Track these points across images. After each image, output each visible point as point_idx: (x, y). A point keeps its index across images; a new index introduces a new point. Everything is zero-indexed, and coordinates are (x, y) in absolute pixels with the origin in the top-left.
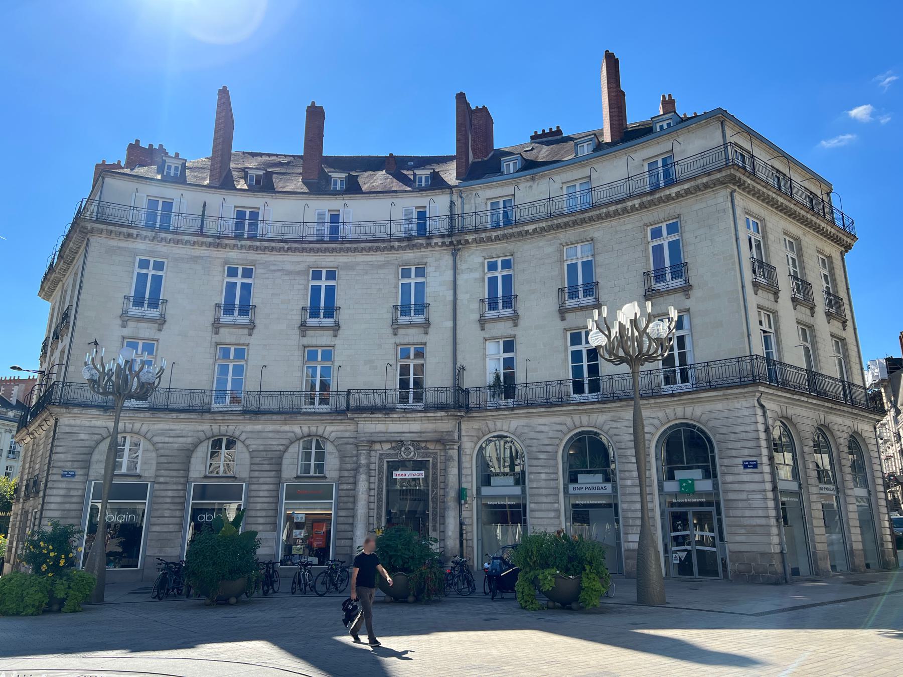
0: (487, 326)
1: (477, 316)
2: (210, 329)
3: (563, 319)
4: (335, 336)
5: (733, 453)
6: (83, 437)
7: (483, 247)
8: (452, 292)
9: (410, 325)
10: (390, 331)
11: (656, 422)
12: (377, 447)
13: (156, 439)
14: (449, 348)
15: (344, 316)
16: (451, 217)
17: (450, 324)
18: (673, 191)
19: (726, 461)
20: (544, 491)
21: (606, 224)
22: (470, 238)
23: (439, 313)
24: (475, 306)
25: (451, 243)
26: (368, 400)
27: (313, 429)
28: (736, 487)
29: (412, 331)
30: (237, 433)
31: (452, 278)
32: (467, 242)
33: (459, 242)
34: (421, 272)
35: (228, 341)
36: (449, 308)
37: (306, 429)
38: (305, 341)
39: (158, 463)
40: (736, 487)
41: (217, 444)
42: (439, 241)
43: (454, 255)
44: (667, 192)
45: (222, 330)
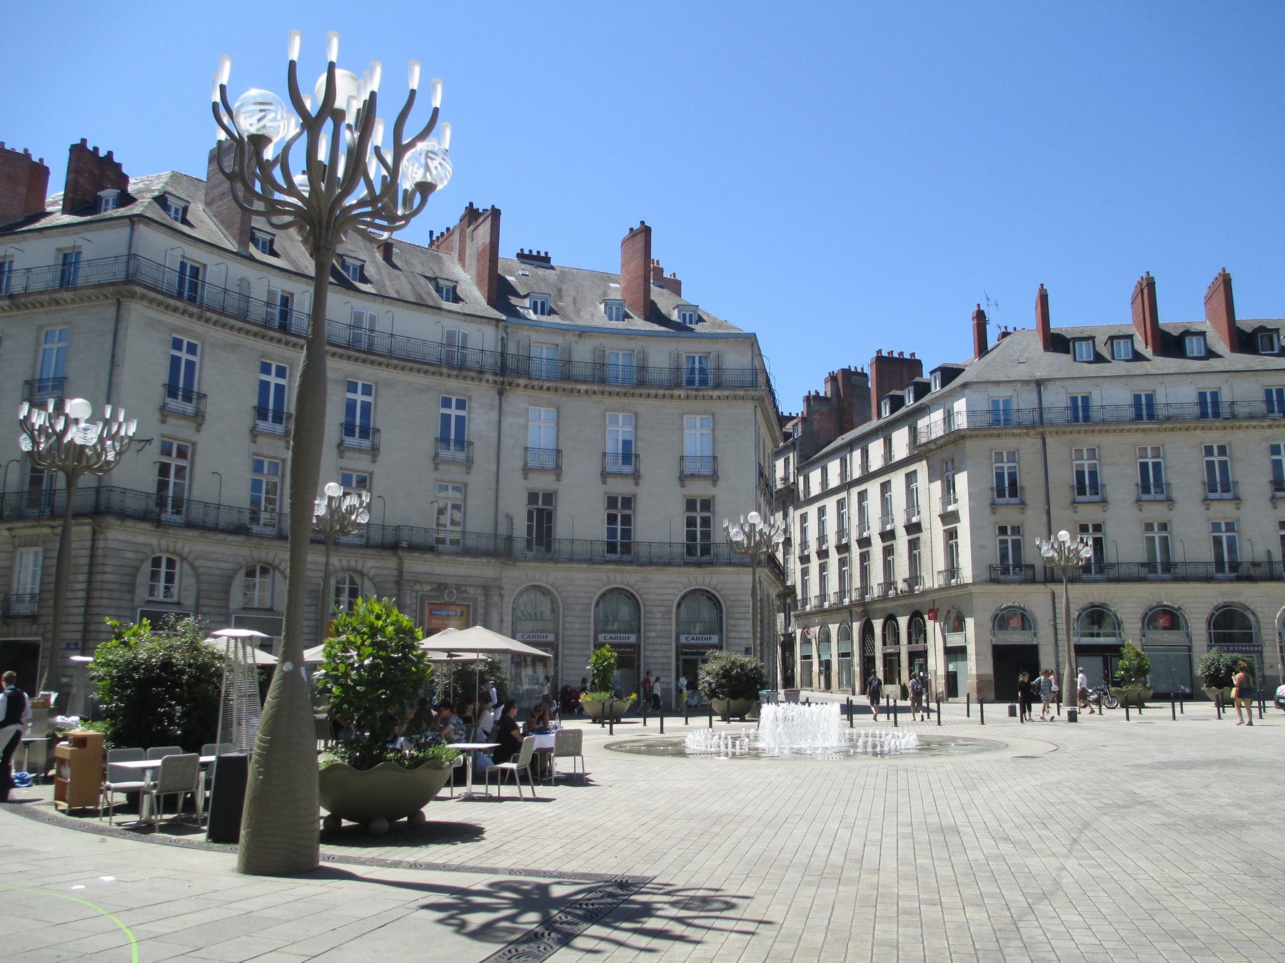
0: (531, 475)
1: (520, 464)
2: (247, 435)
3: (604, 482)
4: (374, 462)
5: (738, 616)
6: (129, 555)
7: (530, 392)
8: (496, 434)
9: (453, 462)
10: (432, 465)
11: (680, 586)
12: (418, 587)
13: (198, 563)
14: (492, 493)
15: (385, 440)
16: (502, 354)
17: (494, 467)
18: (716, 393)
19: (732, 622)
20: (577, 639)
21: (650, 402)
22: (522, 382)
23: (482, 454)
24: (520, 453)
25: (503, 383)
26: (418, 538)
27: (353, 563)
28: (738, 641)
29: (453, 468)
30: (277, 562)
31: (497, 419)
32: (518, 385)
33: (510, 384)
34: (461, 405)
35: (265, 453)
36: (494, 450)
37: (345, 563)
38: (345, 463)
39: (199, 591)
40: (738, 641)
41: (251, 574)
42: (491, 378)
43: (501, 393)
44: (710, 393)
45: (260, 439)
